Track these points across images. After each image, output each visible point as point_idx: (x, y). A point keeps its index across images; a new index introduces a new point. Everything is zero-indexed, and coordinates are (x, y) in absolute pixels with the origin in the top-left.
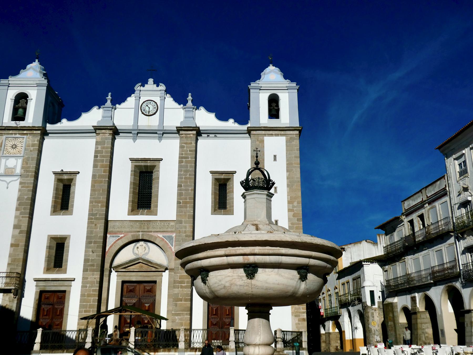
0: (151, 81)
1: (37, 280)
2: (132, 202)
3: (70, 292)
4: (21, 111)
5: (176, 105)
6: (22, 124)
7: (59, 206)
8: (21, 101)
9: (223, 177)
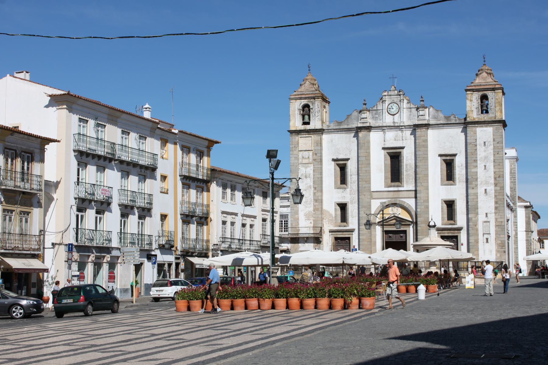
0: (393, 88)
1: (331, 231)
2: (386, 178)
3: (352, 237)
4: (306, 117)
5: (412, 106)
6: (308, 127)
7: (339, 182)
8: (305, 109)
9: (448, 158)
